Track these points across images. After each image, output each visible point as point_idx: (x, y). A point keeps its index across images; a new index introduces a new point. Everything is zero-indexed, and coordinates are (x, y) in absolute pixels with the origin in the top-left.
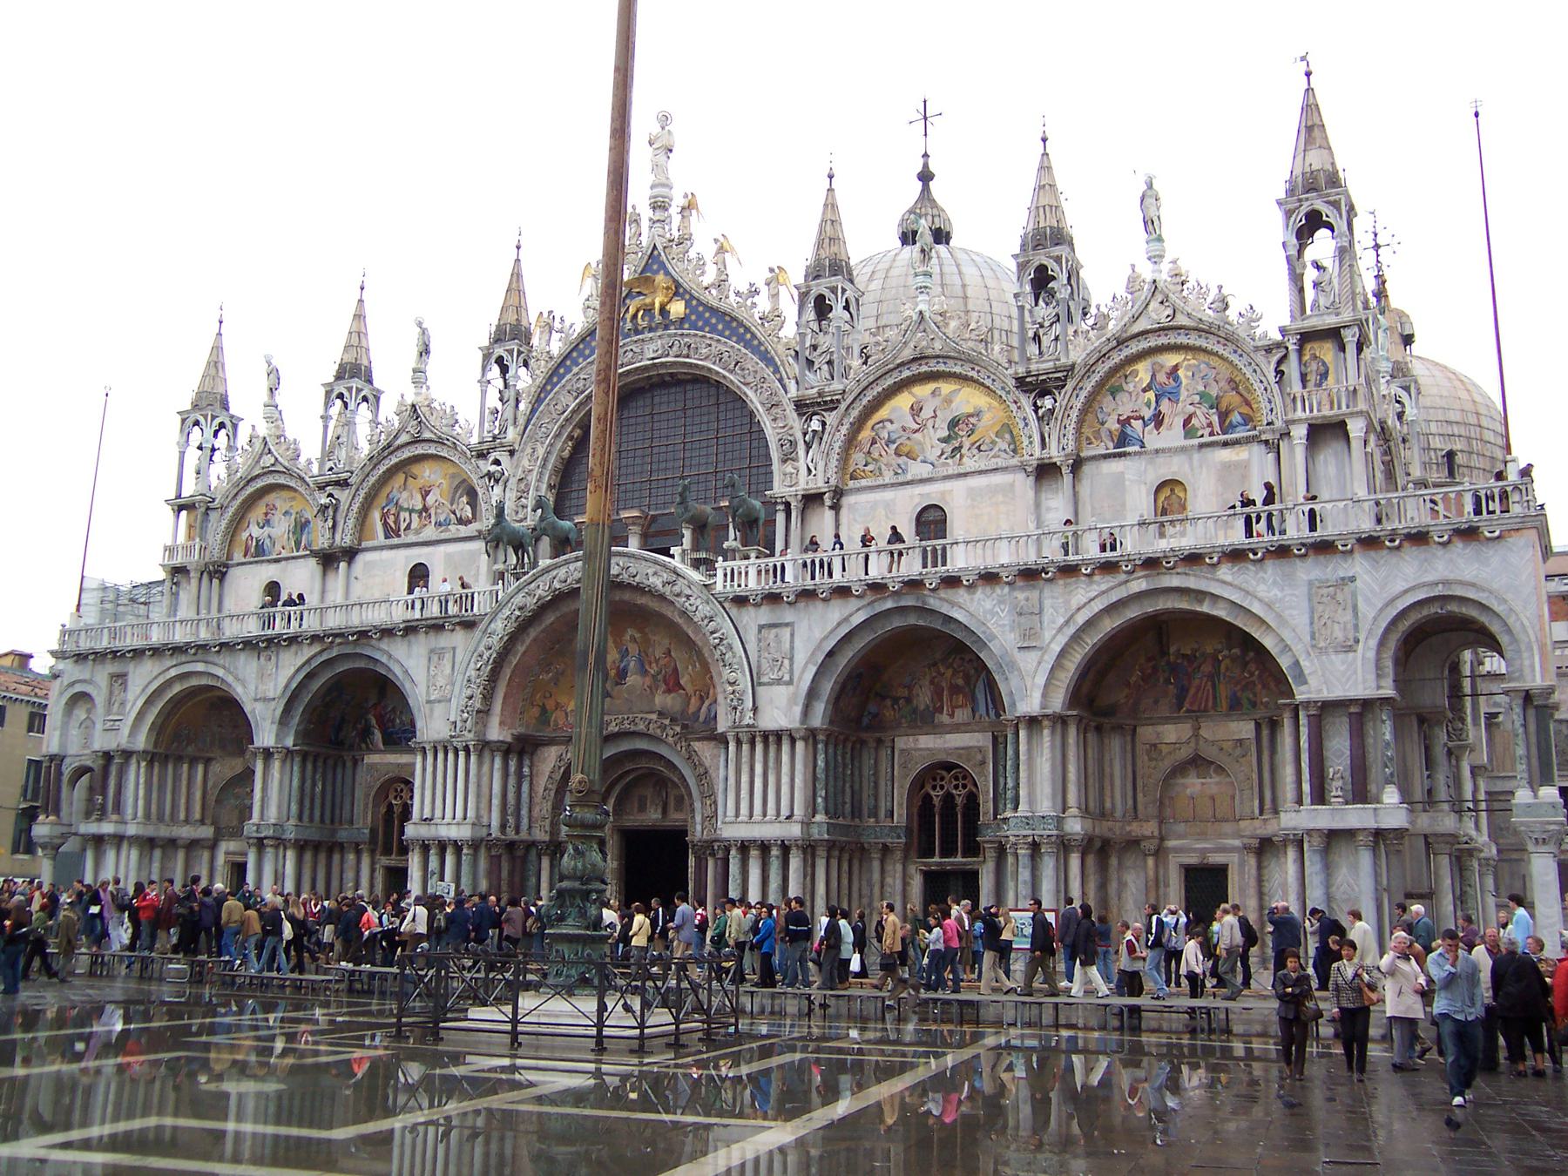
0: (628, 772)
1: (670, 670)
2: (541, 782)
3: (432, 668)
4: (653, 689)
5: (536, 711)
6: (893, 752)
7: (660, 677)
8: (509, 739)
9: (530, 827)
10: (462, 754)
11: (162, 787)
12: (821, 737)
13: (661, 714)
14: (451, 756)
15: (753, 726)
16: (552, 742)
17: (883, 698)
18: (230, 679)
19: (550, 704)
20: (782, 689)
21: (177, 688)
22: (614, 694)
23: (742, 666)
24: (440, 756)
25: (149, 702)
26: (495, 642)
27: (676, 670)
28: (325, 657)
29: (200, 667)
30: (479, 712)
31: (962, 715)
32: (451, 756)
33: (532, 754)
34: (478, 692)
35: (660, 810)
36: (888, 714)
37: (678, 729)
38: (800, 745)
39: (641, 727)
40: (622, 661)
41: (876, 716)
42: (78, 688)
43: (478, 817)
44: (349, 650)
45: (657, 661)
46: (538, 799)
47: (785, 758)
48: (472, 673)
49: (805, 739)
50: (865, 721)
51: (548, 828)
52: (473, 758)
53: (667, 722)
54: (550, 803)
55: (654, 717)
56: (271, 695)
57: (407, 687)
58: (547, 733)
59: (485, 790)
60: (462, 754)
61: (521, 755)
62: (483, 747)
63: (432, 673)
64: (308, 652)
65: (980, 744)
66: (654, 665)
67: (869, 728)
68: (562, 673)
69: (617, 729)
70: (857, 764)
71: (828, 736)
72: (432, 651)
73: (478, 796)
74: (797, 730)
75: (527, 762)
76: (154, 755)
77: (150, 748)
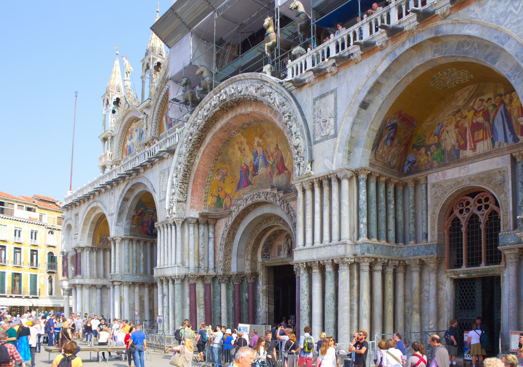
0: (266, 230)
1: (279, 160)
2: (219, 240)
3: (161, 182)
4: (271, 174)
5: (215, 200)
6: (426, 188)
7: (275, 166)
8: (197, 216)
9: (215, 268)
10: (173, 227)
11: (97, 262)
12: (363, 176)
13: (272, 187)
14: (169, 228)
15: (309, 175)
16: (222, 217)
17: (418, 148)
18: (102, 208)
19: (222, 195)
20: (330, 142)
21: (93, 216)
22: (252, 182)
23: (303, 134)
24: (166, 229)
25: (85, 224)
26: (182, 159)
27: (282, 158)
28: (129, 187)
29: (94, 205)
30: (179, 201)
31: (483, 146)
32: (169, 228)
33: (215, 225)
34: (177, 190)
35: (286, 252)
36: (423, 159)
37: (281, 195)
38: (345, 183)
39: (263, 199)
40: (255, 160)
41: (415, 162)
42: (68, 222)
43: (183, 263)
44: (134, 182)
45: (272, 155)
46: (218, 251)
47: (335, 196)
48: (174, 179)
49: (350, 179)
50: (406, 168)
51: (222, 268)
52: (178, 229)
53: (276, 192)
54: (222, 252)
55: (269, 190)
56: (113, 212)
57: (153, 194)
58: (221, 211)
59: (186, 247)
60: (173, 227)
61: (207, 224)
62: (183, 223)
63: (161, 185)
64: (122, 186)
65: (500, 166)
66: (271, 158)
67: (409, 173)
68: (226, 175)
69: (251, 202)
70: (400, 201)
71: (369, 176)
72: (161, 173)
73: (183, 250)
74: (341, 170)
75: (211, 230)
76: (92, 248)
77: (90, 245)
